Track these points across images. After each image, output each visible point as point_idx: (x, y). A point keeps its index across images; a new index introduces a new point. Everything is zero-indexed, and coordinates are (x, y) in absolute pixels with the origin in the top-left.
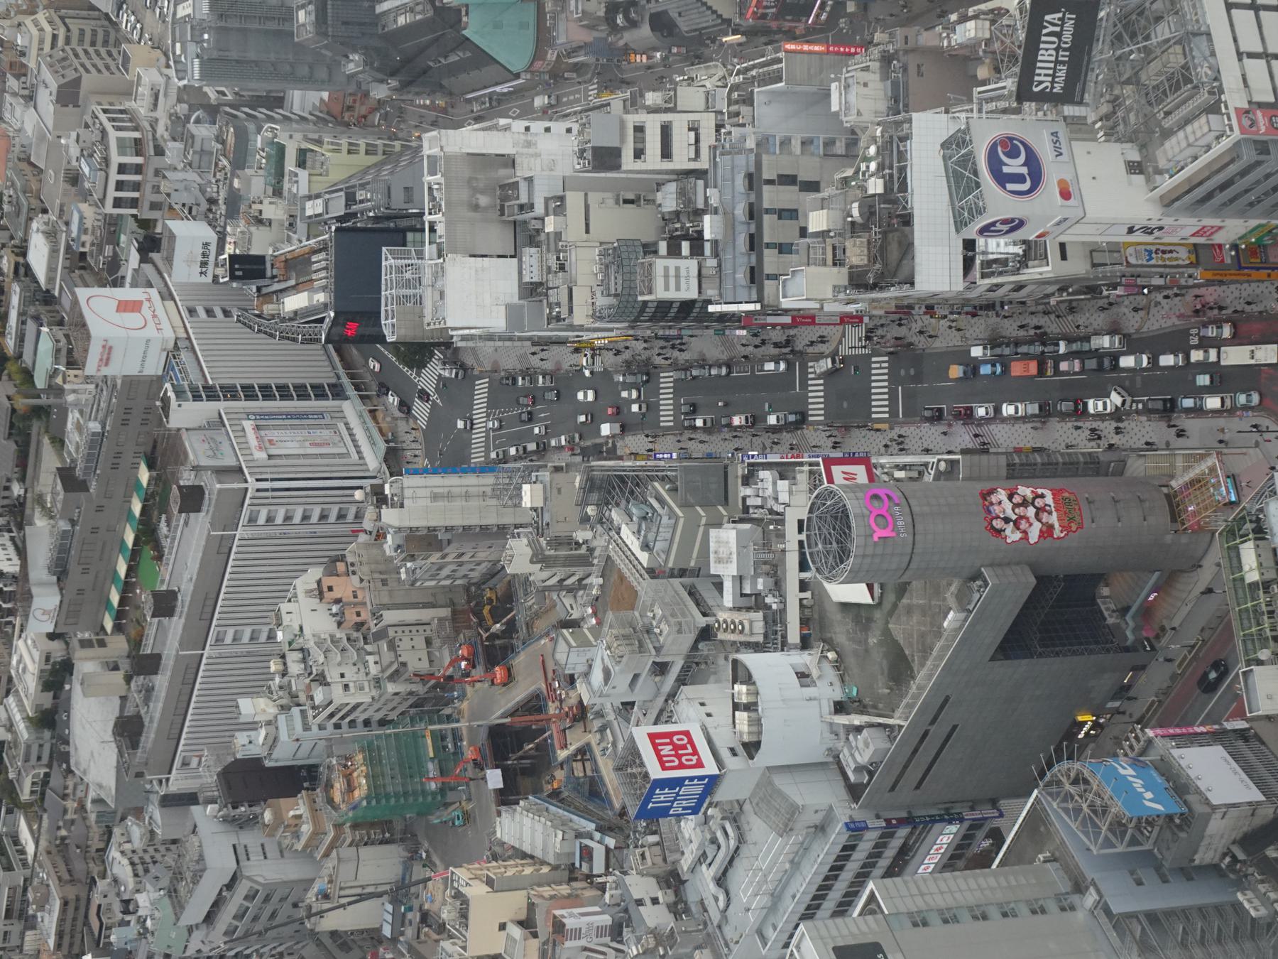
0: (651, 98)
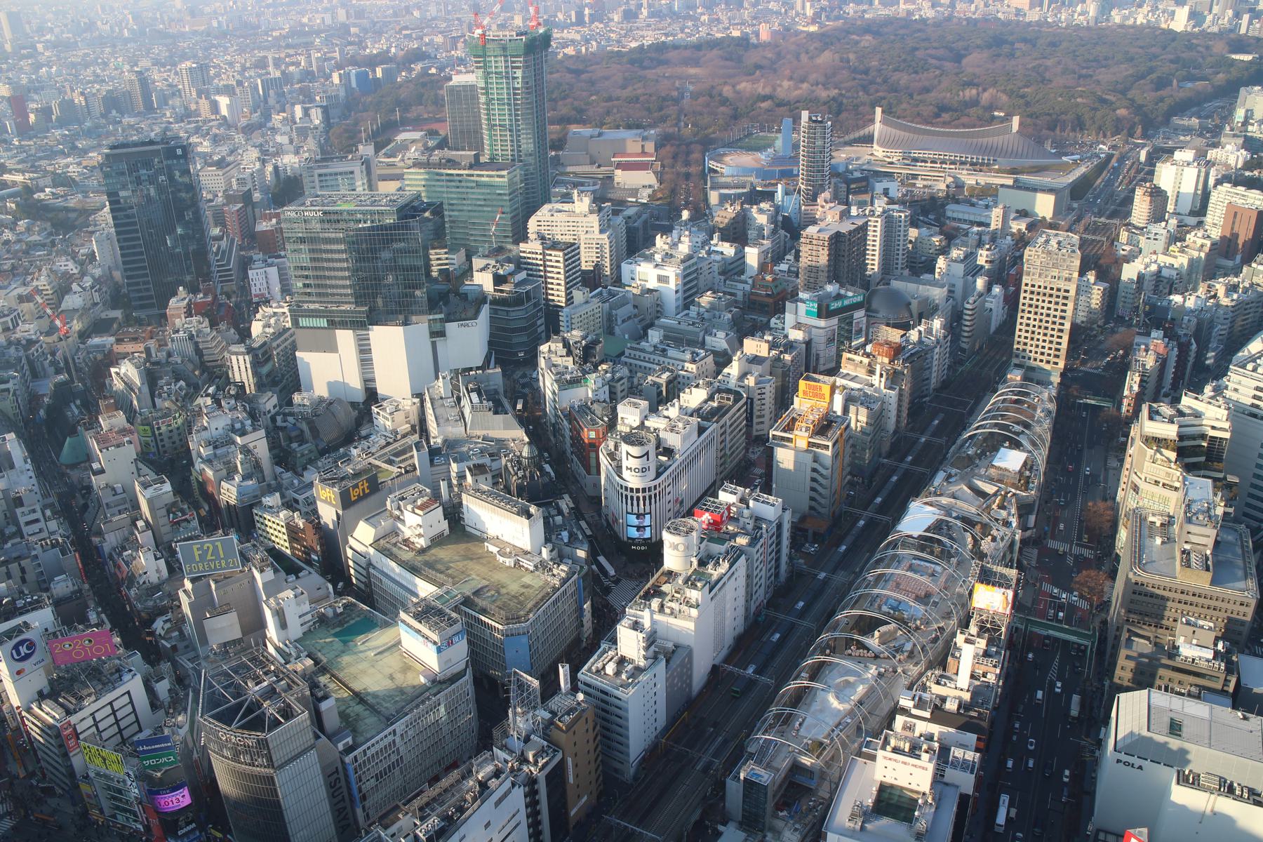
0: (48, 513)
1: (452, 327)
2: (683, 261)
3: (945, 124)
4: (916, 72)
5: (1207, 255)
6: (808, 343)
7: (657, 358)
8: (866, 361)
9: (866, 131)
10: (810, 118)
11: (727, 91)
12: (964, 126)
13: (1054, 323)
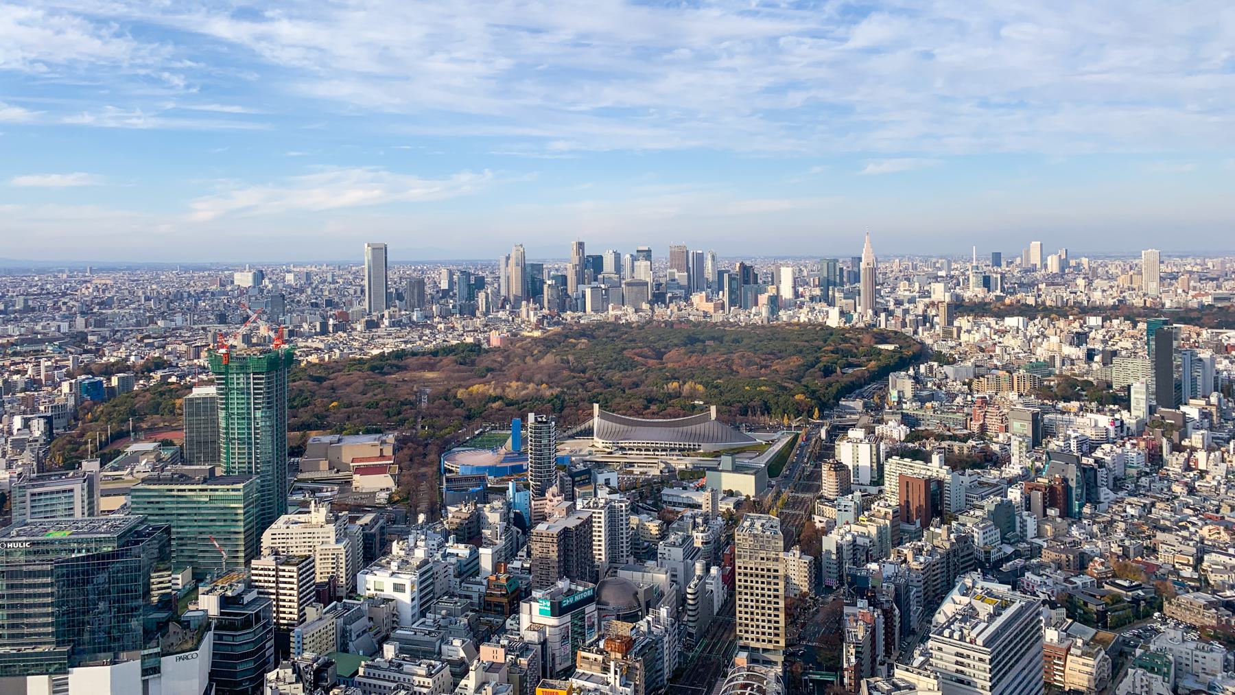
1: (168, 662)
2: (419, 567)
4: (626, 370)
5: (892, 522)
6: (544, 643)
7: (392, 674)
8: (600, 658)
9: (587, 425)
11: (461, 393)
12: (671, 416)
13: (769, 602)
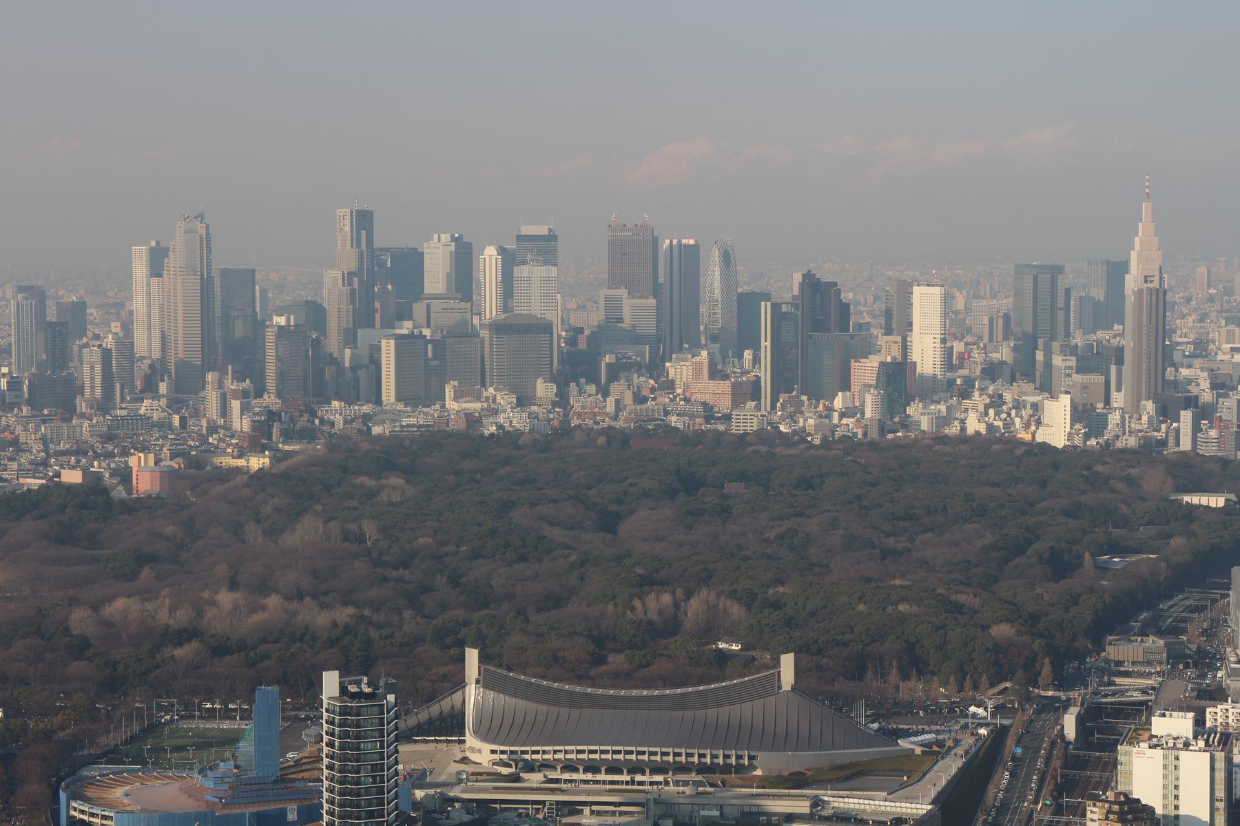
3: (620, 678)
4: (522, 559)
9: (446, 704)
10: (343, 689)
11: (80, 620)
12: (667, 682)
